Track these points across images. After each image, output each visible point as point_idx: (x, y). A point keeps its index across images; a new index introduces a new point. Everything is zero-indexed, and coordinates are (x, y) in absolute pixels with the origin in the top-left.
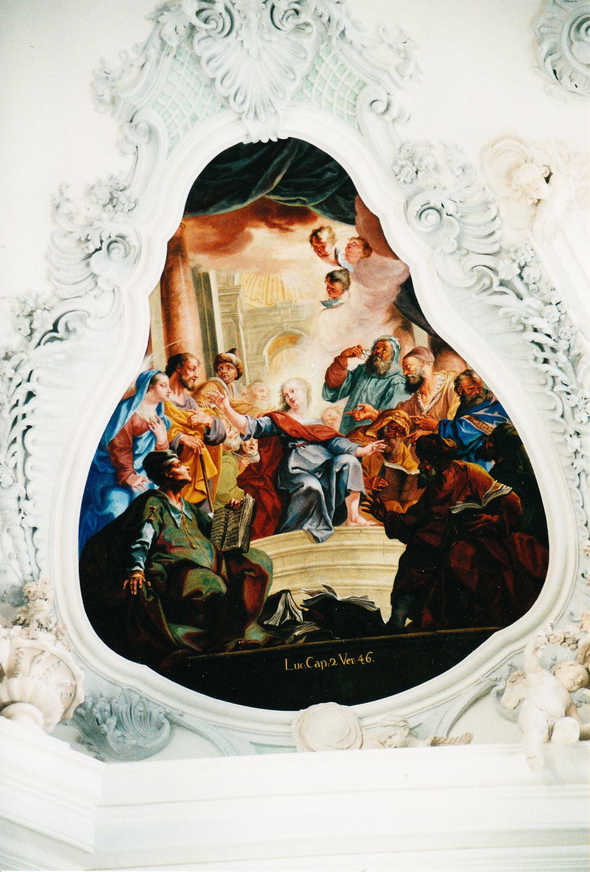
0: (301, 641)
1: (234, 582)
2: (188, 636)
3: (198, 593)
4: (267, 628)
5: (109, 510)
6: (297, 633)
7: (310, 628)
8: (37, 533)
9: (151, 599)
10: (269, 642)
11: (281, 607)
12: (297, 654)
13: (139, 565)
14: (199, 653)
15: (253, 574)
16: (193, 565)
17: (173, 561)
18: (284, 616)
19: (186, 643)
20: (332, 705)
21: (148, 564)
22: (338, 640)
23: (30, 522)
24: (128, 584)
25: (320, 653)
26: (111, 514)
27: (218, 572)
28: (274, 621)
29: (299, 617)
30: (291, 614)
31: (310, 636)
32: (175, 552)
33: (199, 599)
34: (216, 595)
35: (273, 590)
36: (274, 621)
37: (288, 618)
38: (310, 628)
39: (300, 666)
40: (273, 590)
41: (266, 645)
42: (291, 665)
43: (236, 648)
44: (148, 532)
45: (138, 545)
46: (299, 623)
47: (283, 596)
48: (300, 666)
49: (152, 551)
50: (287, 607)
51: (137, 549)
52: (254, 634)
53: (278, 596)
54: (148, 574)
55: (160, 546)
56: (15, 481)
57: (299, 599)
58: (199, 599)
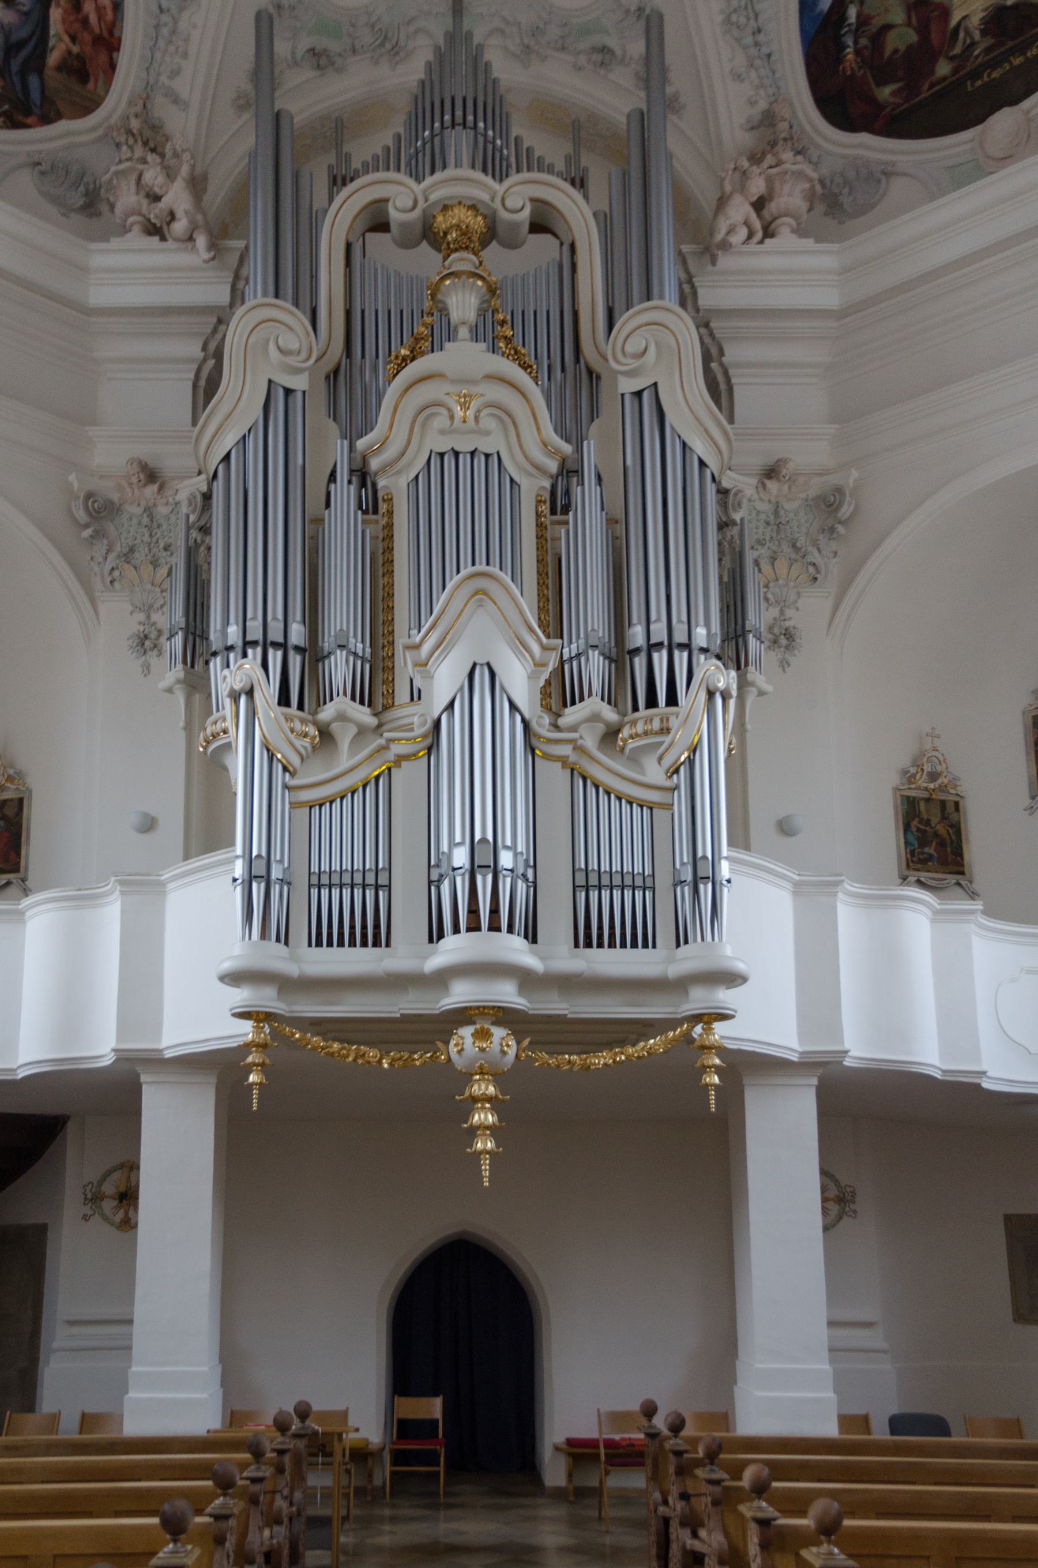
0: (980, 59)
1: (923, 30)
2: (893, 94)
3: (896, 51)
4: (952, 59)
5: (818, 10)
6: (976, 53)
7: (989, 41)
8: (773, 58)
9: (862, 72)
10: (955, 71)
11: (962, 35)
12: (975, 75)
13: (848, 46)
14: (902, 104)
15: (936, 13)
16: (888, 27)
17: (874, 30)
18: (965, 40)
19: (892, 100)
20: (1006, 110)
21: (856, 43)
22: (1010, 44)
23: (765, 50)
24: (844, 68)
25: (993, 64)
26: (822, 11)
27: (909, 24)
28: (957, 50)
29: (977, 35)
30: (972, 38)
31: (988, 50)
32: (874, 21)
33: (898, 56)
34: (910, 48)
35: (954, 21)
36: (957, 50)
37: (968, 41)
38: (989, 41)
39: (979, 83)
40: (954, 21)
41: (953, 75)
42: (972, 85)
43: (930, 88)
44: (852, 13)
45: (846, 29)
46: (978, 42)
47: (963, 25)
48: (979, 83)
49: (857, 30)
50: (968, 32)
51: (846, 33)
52: (943, 69)
53: (959, 25)
54: (858, 52)
55: (863, 20)
56: (748, 19)
57: (975, 21)
58: (898, 56)
